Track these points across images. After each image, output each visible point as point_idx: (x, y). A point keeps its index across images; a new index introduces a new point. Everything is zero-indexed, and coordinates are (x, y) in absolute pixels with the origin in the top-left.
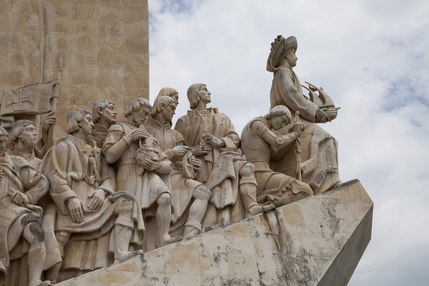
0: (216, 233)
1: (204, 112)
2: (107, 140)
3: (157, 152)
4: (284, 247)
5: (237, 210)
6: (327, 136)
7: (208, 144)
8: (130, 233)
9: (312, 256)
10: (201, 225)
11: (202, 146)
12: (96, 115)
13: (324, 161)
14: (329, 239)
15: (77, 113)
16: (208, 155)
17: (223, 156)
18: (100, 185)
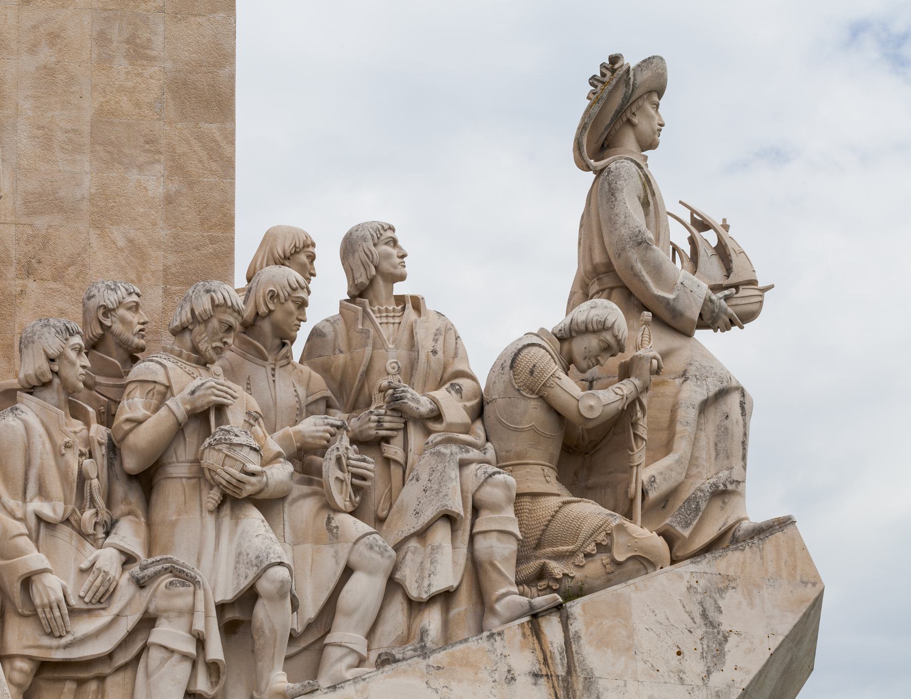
0: (405, 672)
1: (387, 310)
2: (124, 407)
3: (258, 448)
5: (463, 605)
6: (725, 384)
7: (393, 410)
8: (186, 666)
10: (366, 641)
11: (377, 416)
12: (92, 327)
13: (710, 458)
14: (696, 689)
15: (48, 335)
16: (391, 441)
17: (432, 450)
18: (107, 534)
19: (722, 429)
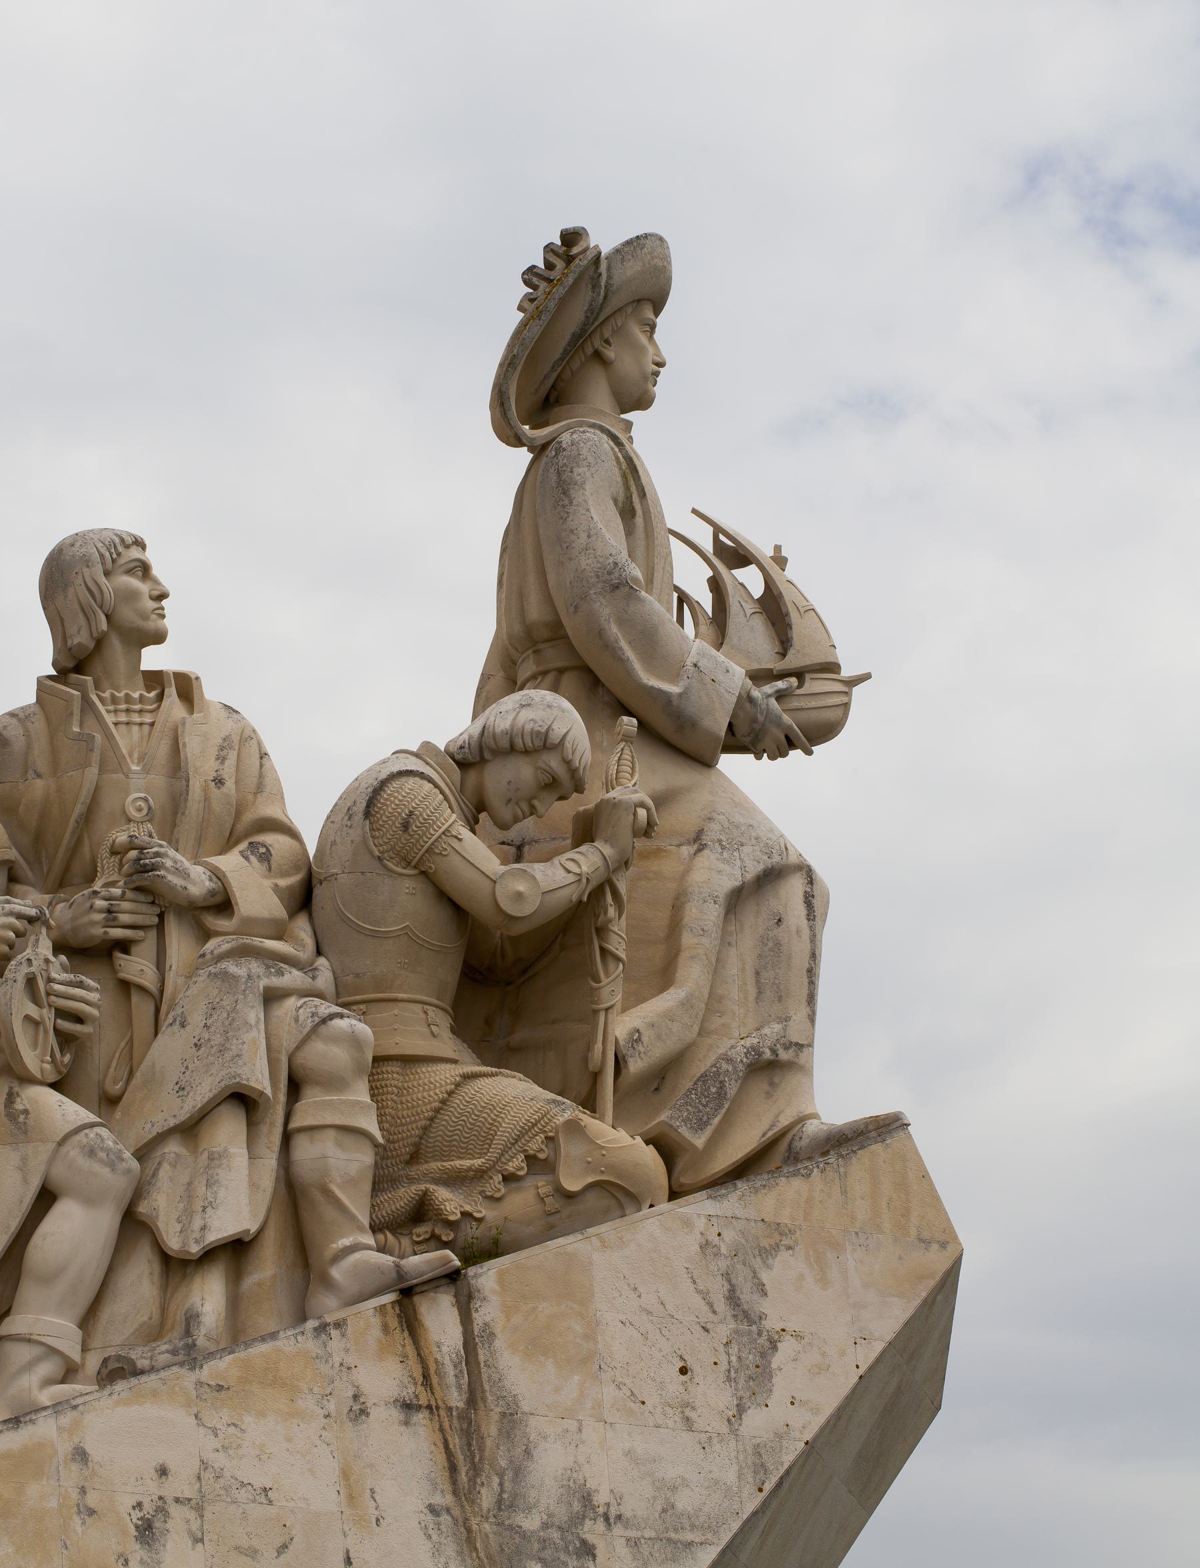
0: (155, 1394)
1: (128, 699)
4: (488, 1477)
6: (776, 859)
7: (138, 889)
9: (619, 1525)
10: (78, 1334)
14: (715, 1440)
16: (134, 949)
19: (770, 944)
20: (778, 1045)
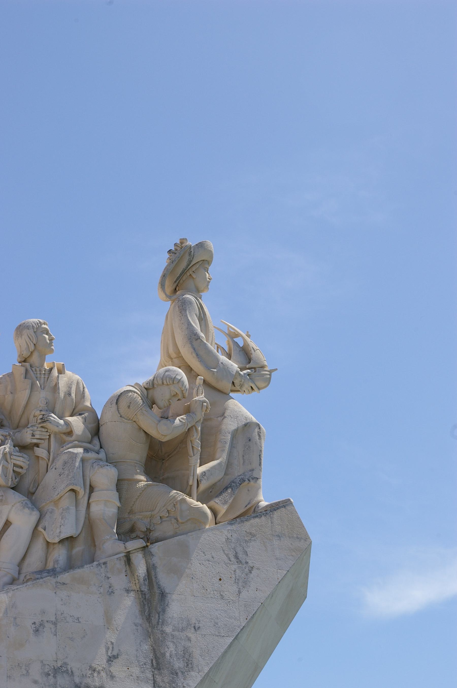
19: (247, 447)
20: (250, 478)
